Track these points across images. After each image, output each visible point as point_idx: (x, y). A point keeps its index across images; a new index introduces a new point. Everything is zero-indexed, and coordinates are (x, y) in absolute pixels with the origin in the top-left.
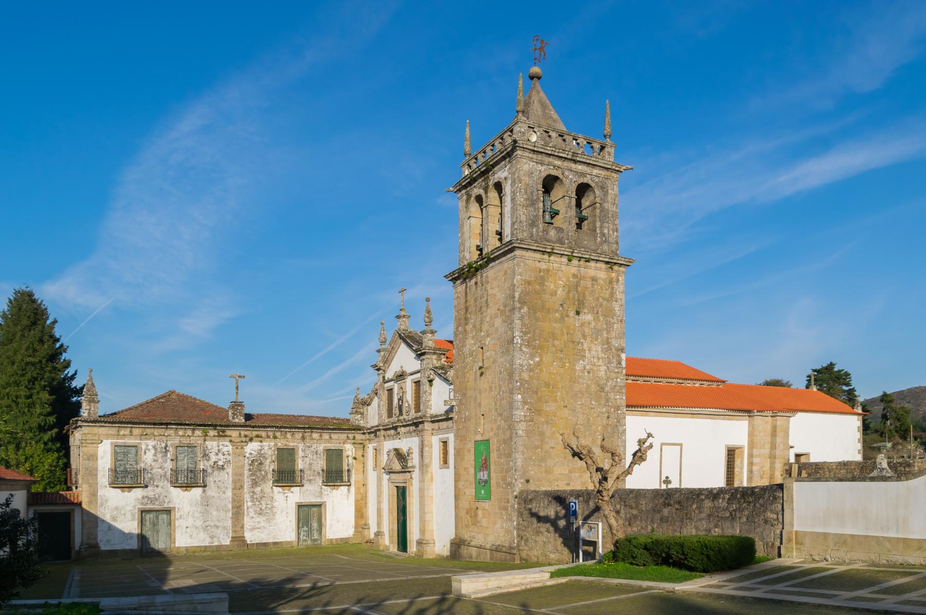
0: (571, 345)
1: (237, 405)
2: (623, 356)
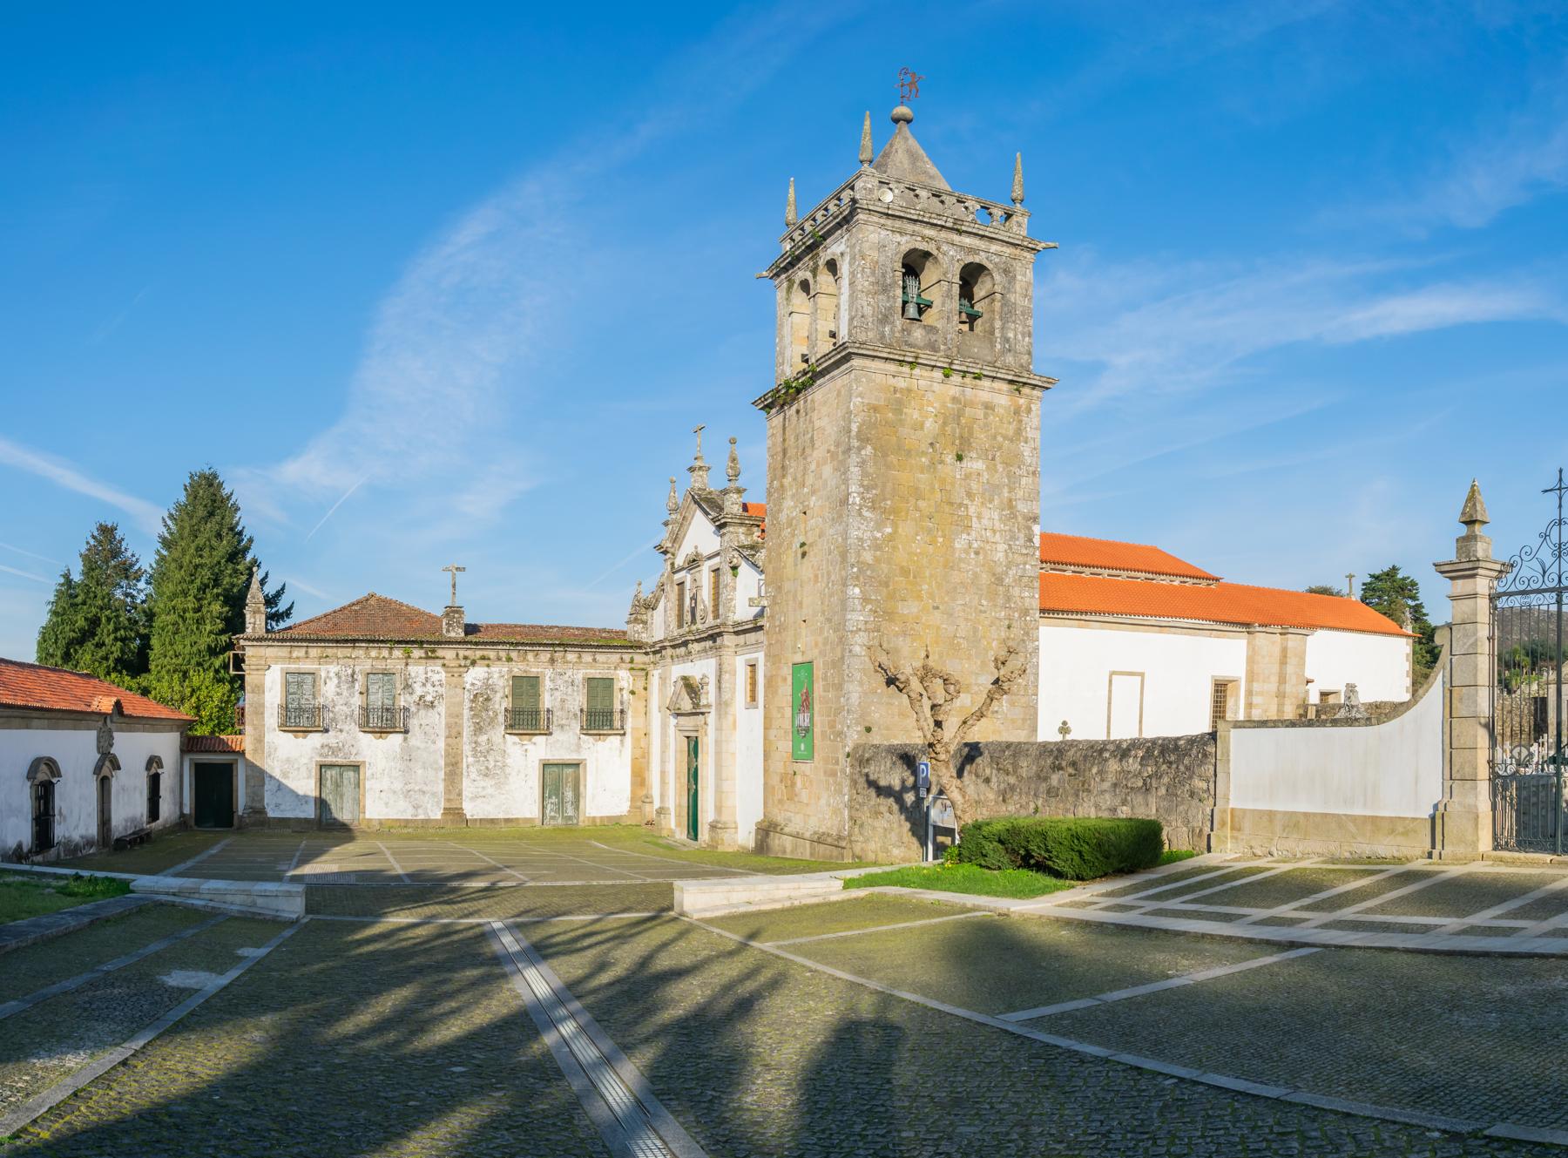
0: (947, 508)
1: (453, 611)
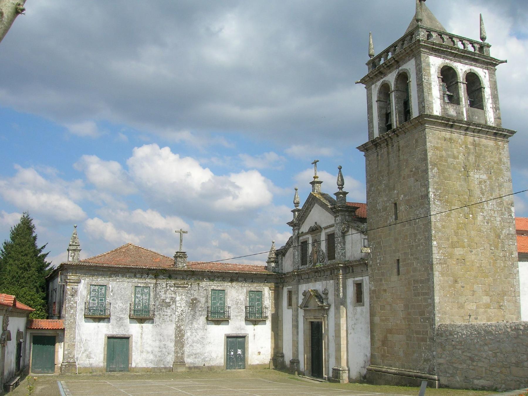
2: (513, 209)
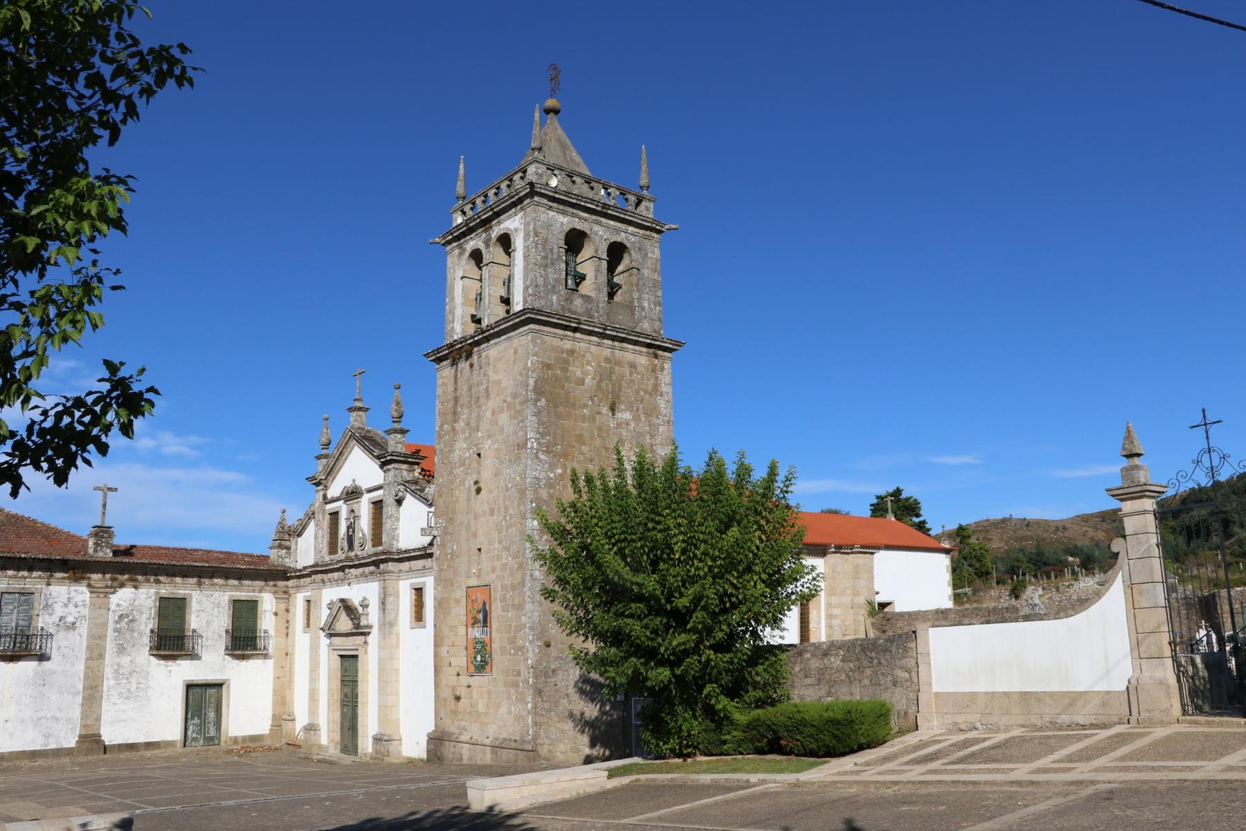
1: (102, 532)
